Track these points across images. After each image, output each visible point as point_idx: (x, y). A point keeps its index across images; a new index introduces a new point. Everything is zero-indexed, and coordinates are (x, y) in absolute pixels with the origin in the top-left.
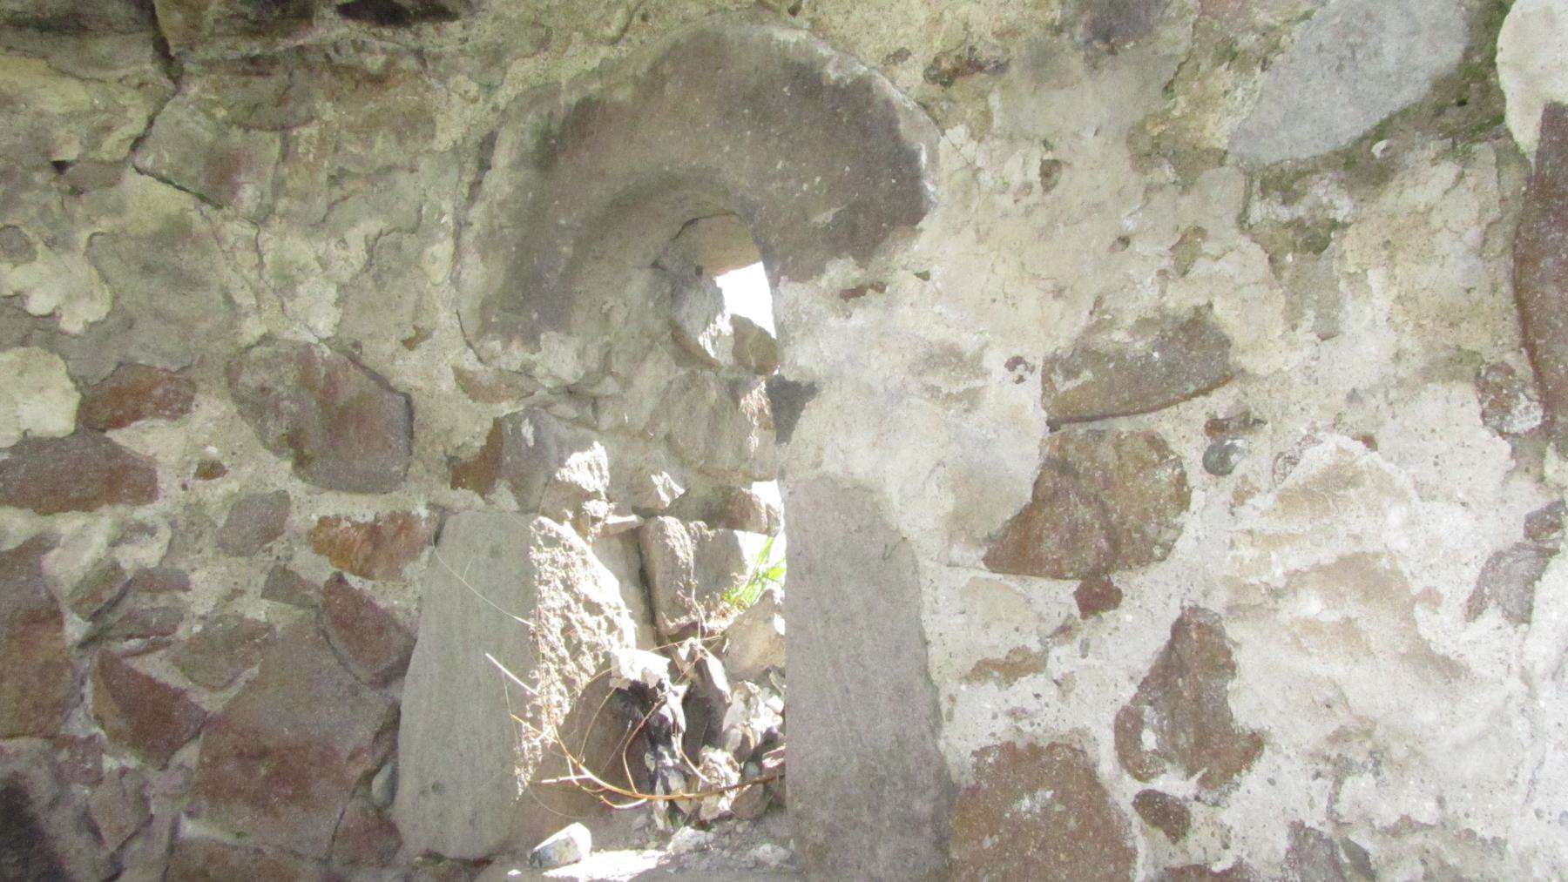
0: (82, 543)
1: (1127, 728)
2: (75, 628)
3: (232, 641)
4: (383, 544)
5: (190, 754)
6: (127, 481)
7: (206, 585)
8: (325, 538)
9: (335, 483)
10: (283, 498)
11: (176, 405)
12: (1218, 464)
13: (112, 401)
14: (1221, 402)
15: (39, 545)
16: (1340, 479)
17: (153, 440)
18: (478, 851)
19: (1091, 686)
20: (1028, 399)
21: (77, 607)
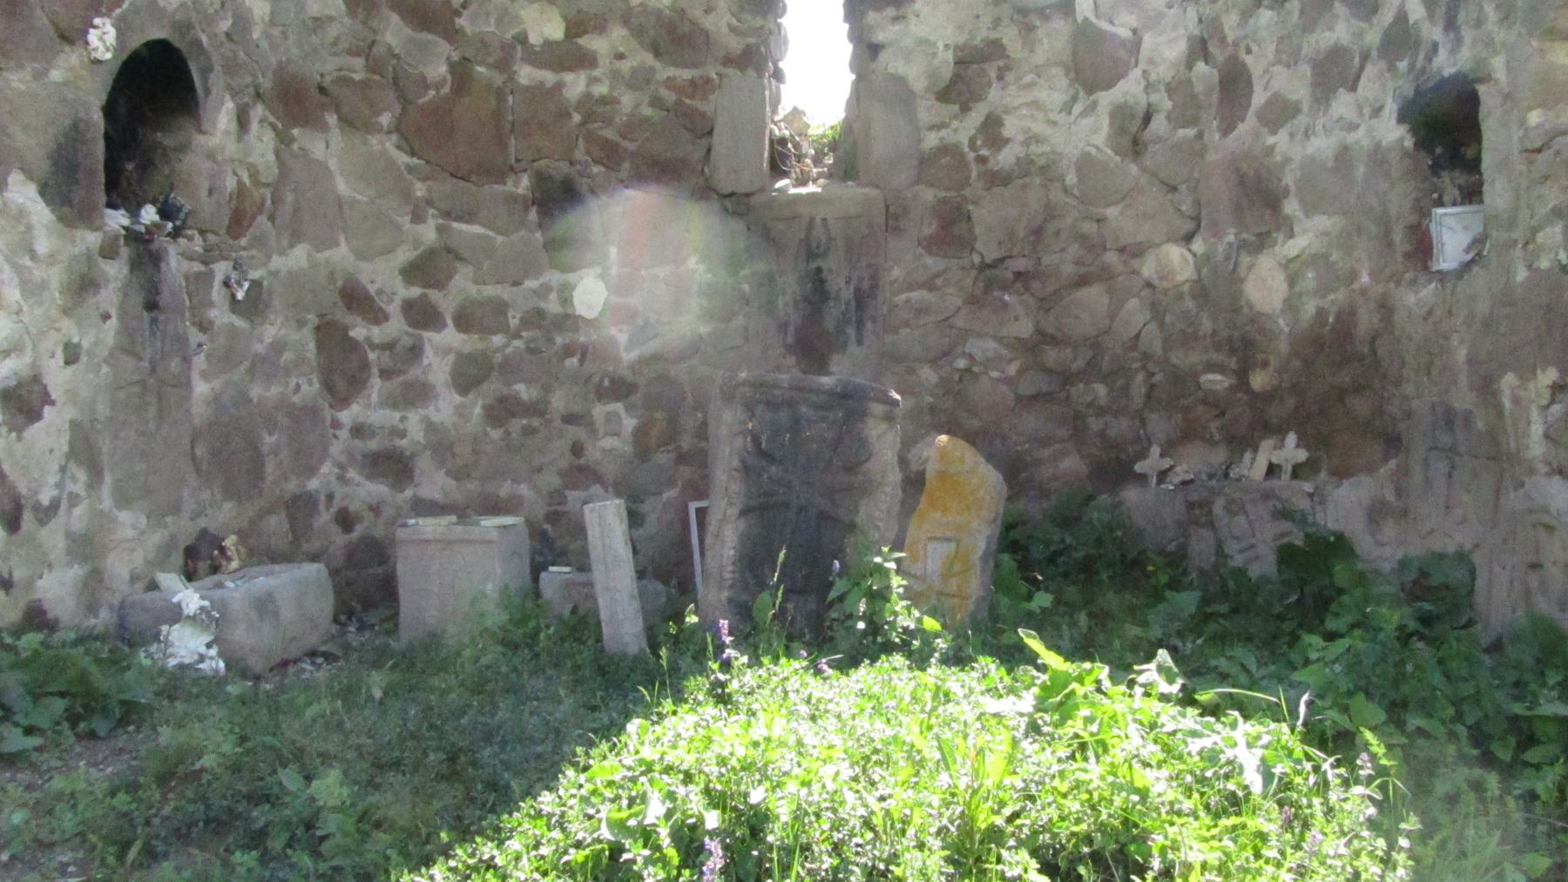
0: (575, 84)
1: (972, 141)
2: (577, 118)
3: (633, 125)
4: (700, 87)
5: (626, 165)
6: (585, 60)
7: (627, 100)
8: (670, 83)
9: (676, 64)
10: (652, 70)
11: (600, 27)
12: (1000, 78)
13: (576, 27)
14: (1001, 63)
15: (559, 86)
16: (1030, 86)
17: (595, 43)
18: (748, 190)
19: (962, 131)
20: (950, 56)
21: (577, 109)
